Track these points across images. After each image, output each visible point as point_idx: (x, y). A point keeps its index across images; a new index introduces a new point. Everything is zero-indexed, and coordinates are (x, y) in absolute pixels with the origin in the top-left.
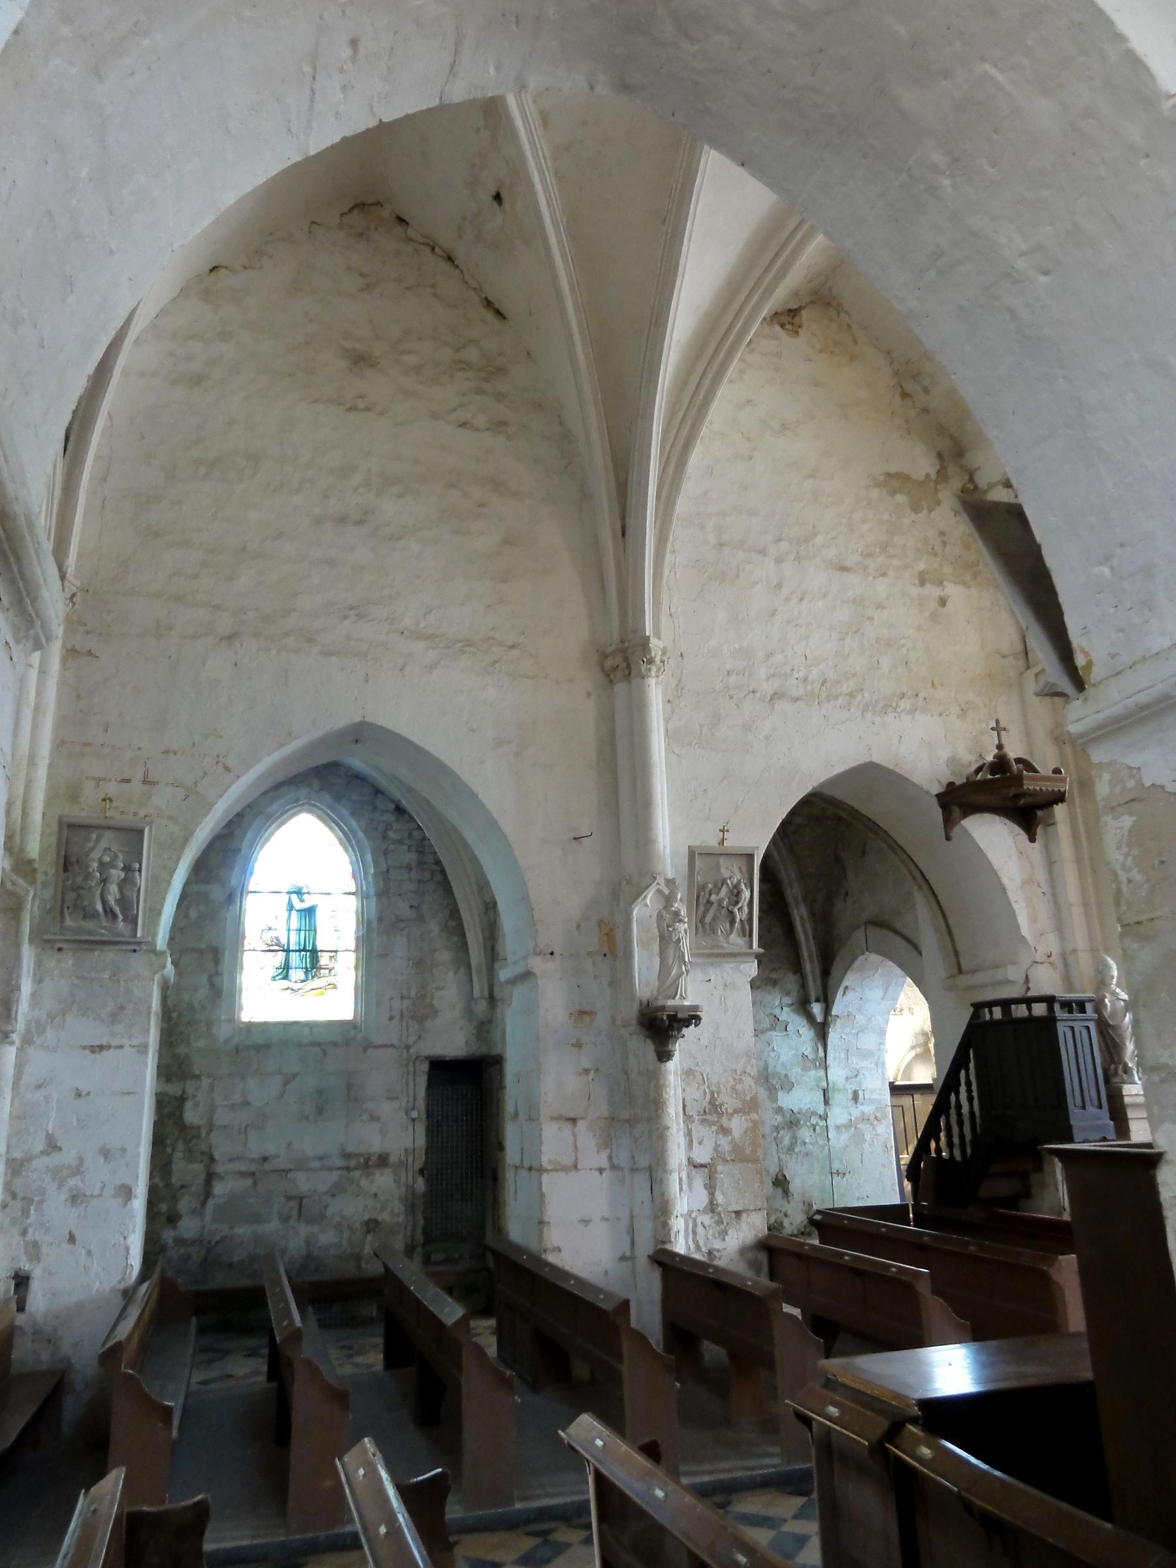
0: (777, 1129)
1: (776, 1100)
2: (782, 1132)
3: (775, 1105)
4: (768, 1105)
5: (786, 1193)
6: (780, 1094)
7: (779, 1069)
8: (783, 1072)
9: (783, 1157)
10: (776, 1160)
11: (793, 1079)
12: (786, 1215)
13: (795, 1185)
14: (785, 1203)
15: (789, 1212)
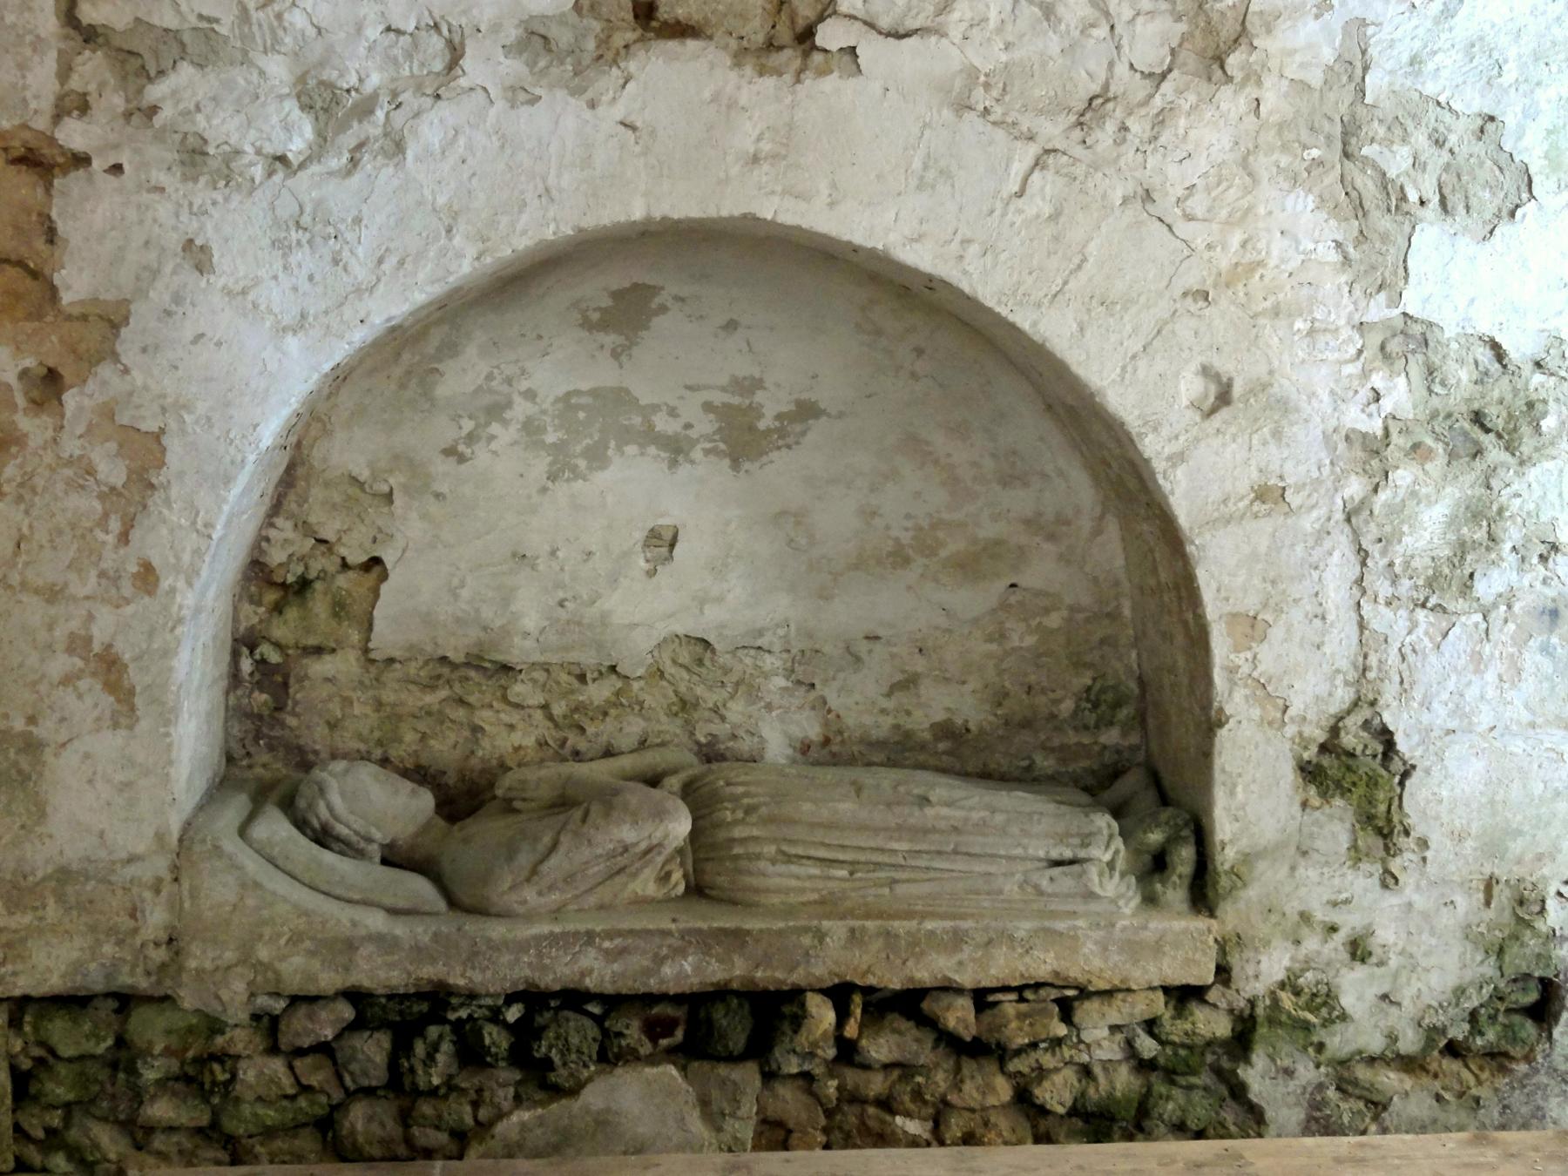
0: (1373, 452)
1: (1390, 283)
2: (1403, 476)
3: (1378, 310)
4: (1338, 304)
5: (1382, 830)
6: (1431, 243)
7: (1446, 77)
8: (1471, 102)
9: (1380, 618)
10: (1341, 644)
11: (1530, 148)
12: (1358, 950)
13: (1448, 790)
14: (1362, 883)
15: (1386, 935)
